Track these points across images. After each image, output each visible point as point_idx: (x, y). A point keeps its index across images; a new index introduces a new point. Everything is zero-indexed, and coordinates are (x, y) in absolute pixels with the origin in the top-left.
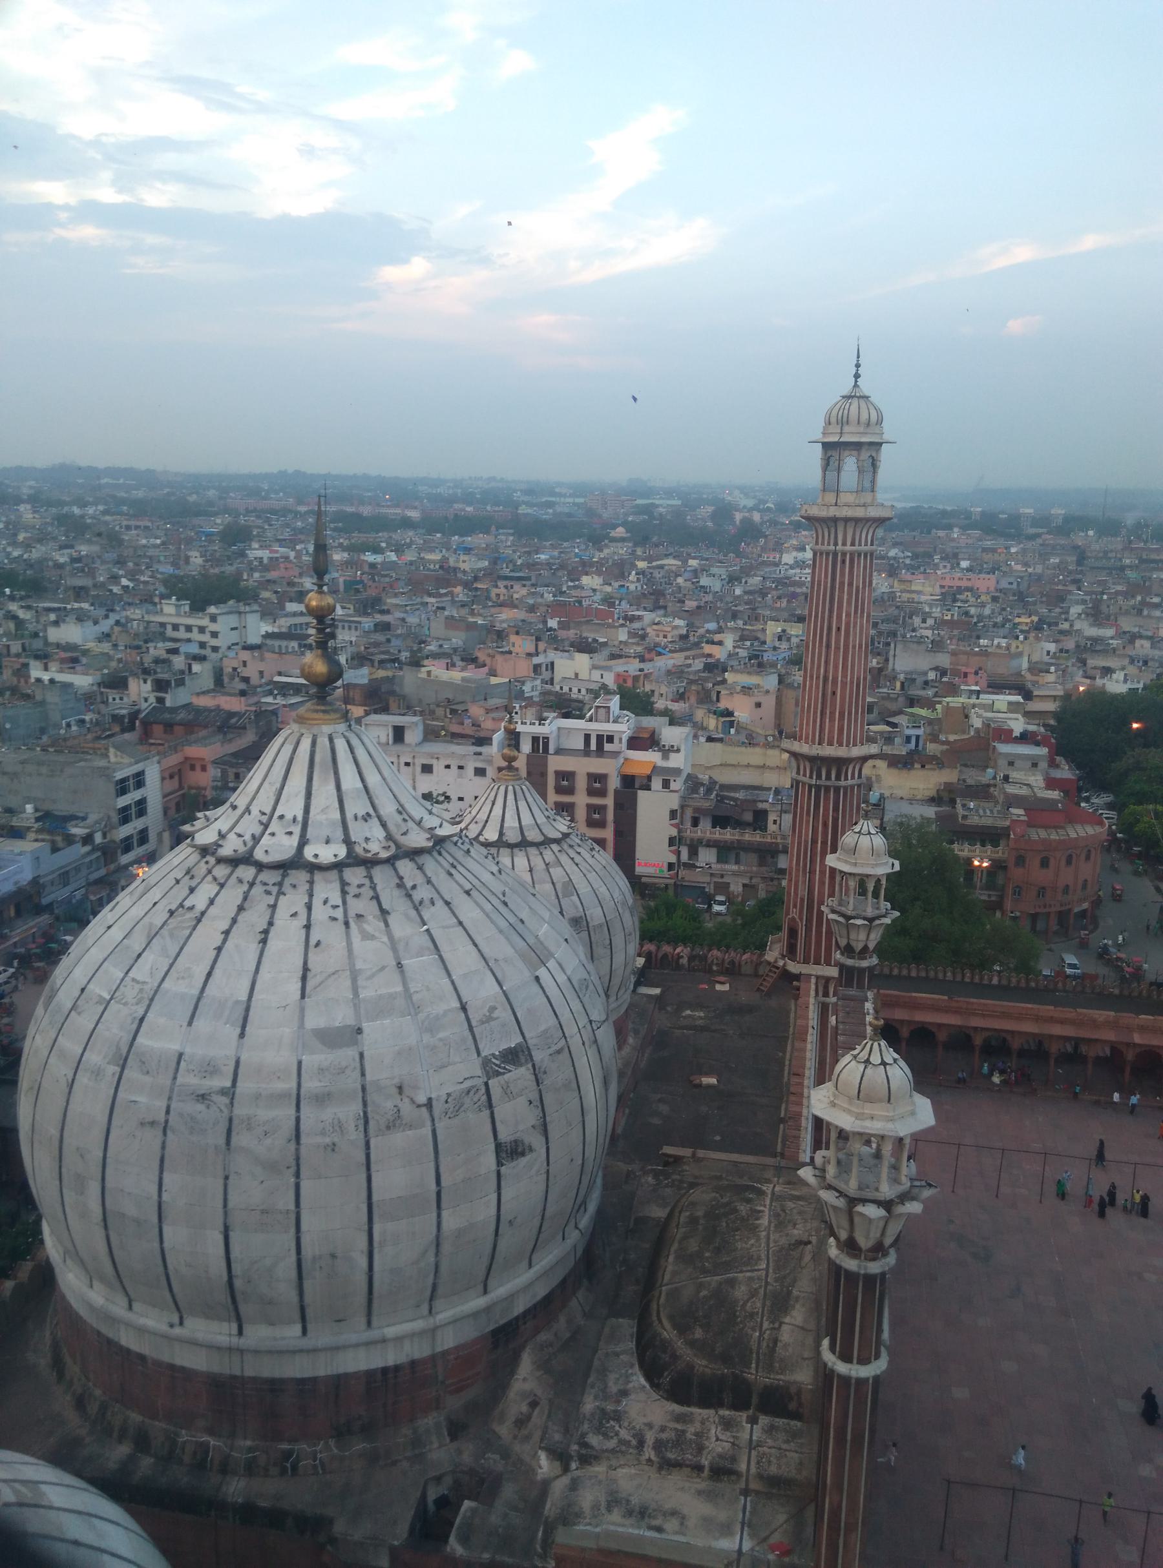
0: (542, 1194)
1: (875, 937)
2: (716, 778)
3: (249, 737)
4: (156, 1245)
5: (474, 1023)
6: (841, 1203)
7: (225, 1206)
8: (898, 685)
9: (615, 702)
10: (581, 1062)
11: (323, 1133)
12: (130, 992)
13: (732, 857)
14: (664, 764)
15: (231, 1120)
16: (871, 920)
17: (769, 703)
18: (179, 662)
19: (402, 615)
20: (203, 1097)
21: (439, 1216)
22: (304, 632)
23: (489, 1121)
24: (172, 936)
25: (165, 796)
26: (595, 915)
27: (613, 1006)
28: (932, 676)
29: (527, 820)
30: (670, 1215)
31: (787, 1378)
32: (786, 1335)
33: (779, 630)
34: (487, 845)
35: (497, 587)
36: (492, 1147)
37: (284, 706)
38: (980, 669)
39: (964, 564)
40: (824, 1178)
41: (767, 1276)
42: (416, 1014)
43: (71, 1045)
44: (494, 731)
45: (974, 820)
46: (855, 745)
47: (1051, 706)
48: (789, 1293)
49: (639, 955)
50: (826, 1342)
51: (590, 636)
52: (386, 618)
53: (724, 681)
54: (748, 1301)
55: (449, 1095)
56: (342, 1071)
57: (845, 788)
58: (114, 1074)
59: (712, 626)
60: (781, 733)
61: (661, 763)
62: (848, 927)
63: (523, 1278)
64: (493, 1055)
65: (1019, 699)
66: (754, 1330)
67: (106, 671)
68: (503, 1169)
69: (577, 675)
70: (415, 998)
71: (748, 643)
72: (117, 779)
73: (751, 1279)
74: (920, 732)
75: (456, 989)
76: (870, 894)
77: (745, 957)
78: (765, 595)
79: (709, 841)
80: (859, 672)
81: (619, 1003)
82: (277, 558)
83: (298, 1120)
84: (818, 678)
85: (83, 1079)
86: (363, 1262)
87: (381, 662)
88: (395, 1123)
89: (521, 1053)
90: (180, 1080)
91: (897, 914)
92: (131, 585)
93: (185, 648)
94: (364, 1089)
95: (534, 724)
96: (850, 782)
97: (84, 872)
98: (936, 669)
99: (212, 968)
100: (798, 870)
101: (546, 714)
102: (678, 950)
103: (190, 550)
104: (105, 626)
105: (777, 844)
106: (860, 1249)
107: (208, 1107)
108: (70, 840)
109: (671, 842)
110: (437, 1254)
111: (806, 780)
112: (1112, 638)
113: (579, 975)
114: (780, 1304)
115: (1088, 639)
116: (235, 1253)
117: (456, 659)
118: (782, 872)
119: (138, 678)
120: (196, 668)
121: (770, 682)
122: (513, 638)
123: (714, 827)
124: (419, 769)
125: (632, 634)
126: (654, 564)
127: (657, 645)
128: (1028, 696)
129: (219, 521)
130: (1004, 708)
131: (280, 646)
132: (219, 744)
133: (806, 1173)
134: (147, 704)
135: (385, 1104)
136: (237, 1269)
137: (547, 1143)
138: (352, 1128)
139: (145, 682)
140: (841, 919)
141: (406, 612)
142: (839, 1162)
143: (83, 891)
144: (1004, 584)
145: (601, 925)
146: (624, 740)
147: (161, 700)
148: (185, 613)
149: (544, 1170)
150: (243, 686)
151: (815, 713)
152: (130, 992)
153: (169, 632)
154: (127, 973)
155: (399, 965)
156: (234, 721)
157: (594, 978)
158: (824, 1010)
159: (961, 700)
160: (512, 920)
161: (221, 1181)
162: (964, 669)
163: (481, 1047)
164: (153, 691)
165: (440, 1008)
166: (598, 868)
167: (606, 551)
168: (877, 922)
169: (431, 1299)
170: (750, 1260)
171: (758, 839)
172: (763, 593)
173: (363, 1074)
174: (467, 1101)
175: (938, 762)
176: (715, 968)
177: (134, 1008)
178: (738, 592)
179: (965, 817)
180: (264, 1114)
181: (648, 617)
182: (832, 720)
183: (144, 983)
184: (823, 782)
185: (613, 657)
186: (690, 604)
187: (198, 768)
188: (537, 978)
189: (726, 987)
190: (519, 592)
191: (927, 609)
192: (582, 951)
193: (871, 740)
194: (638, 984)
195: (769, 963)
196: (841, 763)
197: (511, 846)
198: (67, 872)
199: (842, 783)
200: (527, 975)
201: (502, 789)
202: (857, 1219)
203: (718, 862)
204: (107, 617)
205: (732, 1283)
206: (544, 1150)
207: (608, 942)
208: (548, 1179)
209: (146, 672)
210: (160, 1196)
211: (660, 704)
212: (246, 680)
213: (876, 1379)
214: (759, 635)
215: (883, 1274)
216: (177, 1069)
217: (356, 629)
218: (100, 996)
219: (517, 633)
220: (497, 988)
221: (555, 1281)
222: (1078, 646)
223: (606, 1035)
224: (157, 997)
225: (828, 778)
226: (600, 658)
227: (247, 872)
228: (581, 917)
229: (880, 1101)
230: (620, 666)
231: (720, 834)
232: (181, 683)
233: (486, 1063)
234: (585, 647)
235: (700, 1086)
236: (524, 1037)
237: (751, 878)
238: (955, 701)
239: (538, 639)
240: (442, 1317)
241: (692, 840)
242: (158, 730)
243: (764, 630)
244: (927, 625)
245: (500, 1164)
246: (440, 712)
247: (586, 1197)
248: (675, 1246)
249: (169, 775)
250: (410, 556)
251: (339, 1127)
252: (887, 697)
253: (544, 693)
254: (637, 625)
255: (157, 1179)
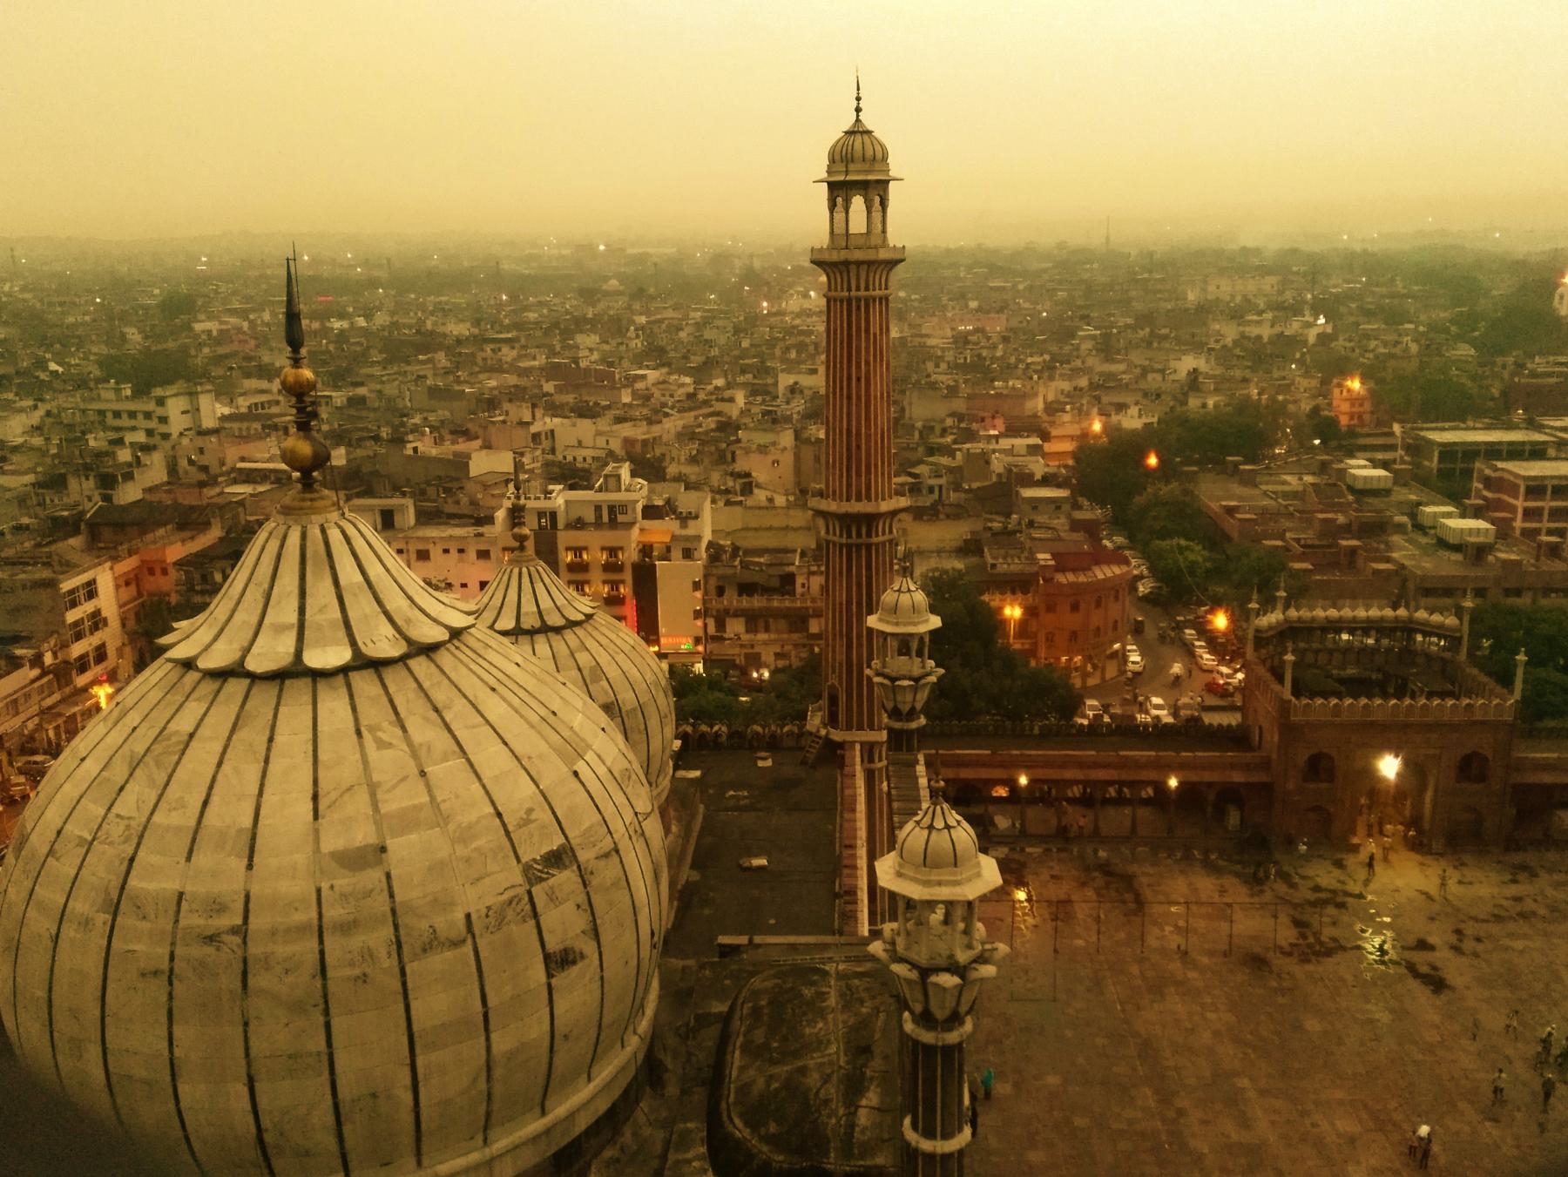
0: (596, 1004)
1: (922, 697)
2: (738, 544)
3: (215, 533)
4: (172, 1105)
5: (511, 828)
6: (914, 975)
7: (247, 1054)
8: (917, 434)
9: (625, 471)
10: (630, 858)
11: (352, 964)
12: (115, 829)
13: (761, 624)
14: (684, 532)
15: (245, 961)
16: (917, 680)
17: (788, 459)
18: (124, 455)
19: (378, 387)
20: (211, 939)
21: (488, 1039)
22: (266, 411)
23: (535, 931)
24: (158, 764)
25: (121, 607)
26: (627, 699)
27: (655, 793)
28: (949, 422)
29: (545, 603)
30: (732, 1007)
31: (869, 1163)
32: (863, 1118)
33: (791, 382)
34: (505, 633)
35: (482, 350)
36: (541, 957)
37: (251, 495)
38: (997, 412)
39: (973, 304)
40: (895, 951)
41: (838, 1059)
42: (447, 825)
43: (50, 894)
44: (495, 509)
45: (1003, 568)
46: (883, 499)
47: (1068, 446)
48: (863, 1074)
49: (676, 738)
50: (907, 1121)
51: (592, 400)
52: (362, 391)
53: (738, 441)
54: (821, 1087)
55: (489, 908)
56: (368, 894)
57: (877, 545)
58: (105, 923)
59: (720, 382)
60: (804, 492)
61: (679, 532)
62: (895, 689)
63: (585, 1092)
64: (534, 860)
65: (1035, 440)
66: (829, 1117)
67: (39, 469)
68: (554, 981)
69: (580, 442)
70: (443, 807)
71: (759, 399)
72: (64, 590)
73: (821, 1065)
74: (943, 481)
75: (487, 793)
76: (914, 654)
77: (786, 729)
78: (774, 347)
79: (736, 610)
80: (883, 423)
81: (659, 790)
82: (228, 330)
83: (322, 953)
84: (841, 432)
85: (69, 931)
86: (408, 1098)
87: (360, 439)
88: (433, 943)
89: (564, 856)
90: (182, 923)
91: (941, 671)
92: (61, 370)
93: (129, 438)
94: (393, 911)
95: (539, 498)
96: (881, 539)
97: (35, 698)
98: (952, 415)
99: (208, 795)
100: (834, 635)
101: (551, 487)
102: (716, 728)
103: (126, 325)
104: (36, 417)
105: (807, 608)
106: (936, 1021)
107: (218, 949)
108: (15, 664)
109: (697, 614)
110: (489, 1078)
111: (836, 539)
112: (1124, 373)
113: (619, 766)
114: (854, 1087)
115: (1101, 374)
116: (263, 1102)
117: (445, 433)
118: (818, 636)
119: (79, 476)
120: (145, 459)
121: (787, 438)
122: (506, 406)
123: (740, 595)
124: (413, 556)
125: (635, 394)
126: (653, 318)
127: (664, 405)
128: (1045, 437)
129: (157, 291)
130: (1024, 451)
131: (240, 429)
132: (179, 544)
133: (876, 948)
134: (91, 504)
135: (414, 928)
136: (266, 1122)
137: (599, 947)
138: (383, 953)
139: (87, 479)
140: (886, 682)
141: (383, 382)
142: (908, 934)
143: (36, 720)
144: (1014, 323)
145: (634, 709)
146: (639, 507)
147: (107, 498)
148: (127, 397)
149: (597, 977)
150: (203, 477)
151: (841, 470)
152: (115, 829)
153: (110, 420)
154: (109, 809)
155: (423, 774)
156: (195, 516)
157: (636, 766)
158: (870, 777)
159: (981, 445)
160: (543, 712)
161: (241, 1029)
162: (981, 414)
163: (520, 852)
164: (97, 488)
165: (472, 817)
166: (627, 648)
167: (601, 306)
168: (923, 681)
169: (486, 1128)
170: (820, 1043)
171: (787, 604)
172: (771, 343)
173: (392, 896)
174: (510, 914)
175: (957, 513)
176: (755, 744)
177: (122, 847)
178: (745, 344)
179: (993, 566)
180: (282, 950)
181: (653, 375)
182: (859, 475)
183: (129, 818)
184: (854, 540)
185: (619, 420)
186: (696, 360)
187: (158, 571)
188: (576, 774)
189: (769, 763)
190: (508, 354)
191: (939, 353)
192: (620, 738)
193: (900, 493)
194: (676, 768)
195: (811, 734)
196: (870, 520)
197: (532, 633)
198: (15, 701)
199: (875, 540)
200: (565, 770)
201: (516, 571)
202: (931, 992)
203: (747, 631)
204: (36, 407)
205: (803, 1071)
206: (596, 956)
207: (643, 727)
208: (602, 986)
209: (86, 469)
210: (171, 1052)
211: (672, 470)
212: (205, 469)
213: (961, 1152)
214: (771, 389)
215: (960, 1044)
216: (178, 912)
217: (327, 404)
218: (80, 837)
219: (510, 401)
220: (534, 787)
221: (617, 1092)
222: (1091, 383)
223: (653, 827)
224: (147, 834)
225: (859, 535)
226: (603, 424)
227: (236, 687)
228: (612, 703)
229: (947, 866)
230: (627, 430)
231: (745, 602)
232: (129, 477)
233: (527, 869)
234: (585, 412)
235: (750, 869)
236: (566, 837)
237: (783, 646)
238: (975, 447)
239: (534, 406)
240: (500, 1144)
241: (718, 611)
242: (107, 533)
243: (776, 384)
244: (940, 370)
245: (550, 975)
246: (431, 491)
247: (643, 999)
248: (741, 1038)
249: (123, 582)
250: (381, 319)
251: (368, 954)
252: (908, 448)
253: (547, 464)
254: (639, 385)
255: (165, 1033)
